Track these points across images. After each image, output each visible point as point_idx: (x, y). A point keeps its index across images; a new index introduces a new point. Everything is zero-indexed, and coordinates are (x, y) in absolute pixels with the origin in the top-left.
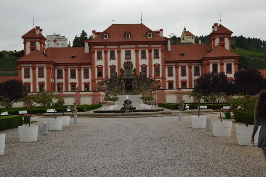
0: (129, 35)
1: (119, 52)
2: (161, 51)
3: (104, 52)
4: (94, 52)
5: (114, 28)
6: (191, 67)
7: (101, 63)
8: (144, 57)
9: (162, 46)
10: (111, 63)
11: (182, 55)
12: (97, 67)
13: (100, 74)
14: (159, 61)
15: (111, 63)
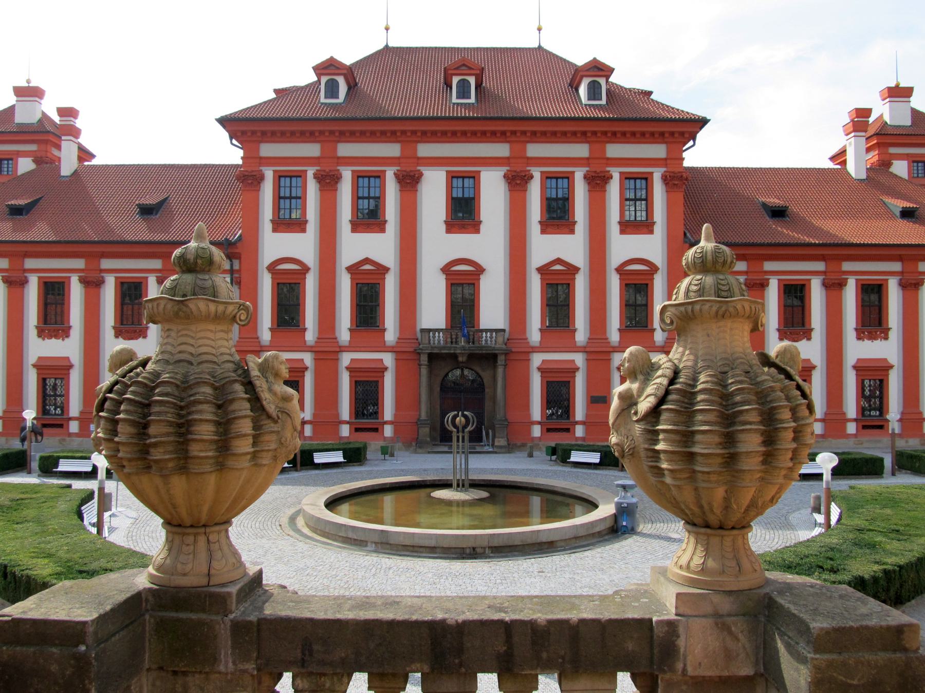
0: (472, 80)
1: (410, 182)
2: (666, 179)
3: (319, 178)
4: (261, 178)
5: (390, 58)
6: (841, 284)
7: (302, 247)
8: (558, 216)
9: (668, 152)
10: (355, 247)
11: (778, 213)
12: (272, 268)
13: (288, 312)
14: (651, 247)
15: (355, 247)
